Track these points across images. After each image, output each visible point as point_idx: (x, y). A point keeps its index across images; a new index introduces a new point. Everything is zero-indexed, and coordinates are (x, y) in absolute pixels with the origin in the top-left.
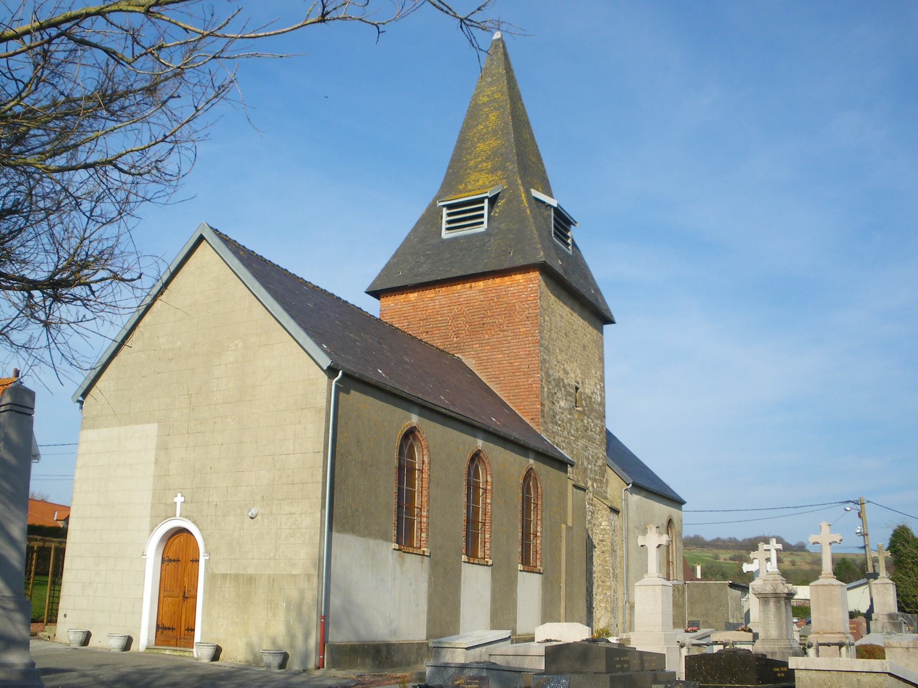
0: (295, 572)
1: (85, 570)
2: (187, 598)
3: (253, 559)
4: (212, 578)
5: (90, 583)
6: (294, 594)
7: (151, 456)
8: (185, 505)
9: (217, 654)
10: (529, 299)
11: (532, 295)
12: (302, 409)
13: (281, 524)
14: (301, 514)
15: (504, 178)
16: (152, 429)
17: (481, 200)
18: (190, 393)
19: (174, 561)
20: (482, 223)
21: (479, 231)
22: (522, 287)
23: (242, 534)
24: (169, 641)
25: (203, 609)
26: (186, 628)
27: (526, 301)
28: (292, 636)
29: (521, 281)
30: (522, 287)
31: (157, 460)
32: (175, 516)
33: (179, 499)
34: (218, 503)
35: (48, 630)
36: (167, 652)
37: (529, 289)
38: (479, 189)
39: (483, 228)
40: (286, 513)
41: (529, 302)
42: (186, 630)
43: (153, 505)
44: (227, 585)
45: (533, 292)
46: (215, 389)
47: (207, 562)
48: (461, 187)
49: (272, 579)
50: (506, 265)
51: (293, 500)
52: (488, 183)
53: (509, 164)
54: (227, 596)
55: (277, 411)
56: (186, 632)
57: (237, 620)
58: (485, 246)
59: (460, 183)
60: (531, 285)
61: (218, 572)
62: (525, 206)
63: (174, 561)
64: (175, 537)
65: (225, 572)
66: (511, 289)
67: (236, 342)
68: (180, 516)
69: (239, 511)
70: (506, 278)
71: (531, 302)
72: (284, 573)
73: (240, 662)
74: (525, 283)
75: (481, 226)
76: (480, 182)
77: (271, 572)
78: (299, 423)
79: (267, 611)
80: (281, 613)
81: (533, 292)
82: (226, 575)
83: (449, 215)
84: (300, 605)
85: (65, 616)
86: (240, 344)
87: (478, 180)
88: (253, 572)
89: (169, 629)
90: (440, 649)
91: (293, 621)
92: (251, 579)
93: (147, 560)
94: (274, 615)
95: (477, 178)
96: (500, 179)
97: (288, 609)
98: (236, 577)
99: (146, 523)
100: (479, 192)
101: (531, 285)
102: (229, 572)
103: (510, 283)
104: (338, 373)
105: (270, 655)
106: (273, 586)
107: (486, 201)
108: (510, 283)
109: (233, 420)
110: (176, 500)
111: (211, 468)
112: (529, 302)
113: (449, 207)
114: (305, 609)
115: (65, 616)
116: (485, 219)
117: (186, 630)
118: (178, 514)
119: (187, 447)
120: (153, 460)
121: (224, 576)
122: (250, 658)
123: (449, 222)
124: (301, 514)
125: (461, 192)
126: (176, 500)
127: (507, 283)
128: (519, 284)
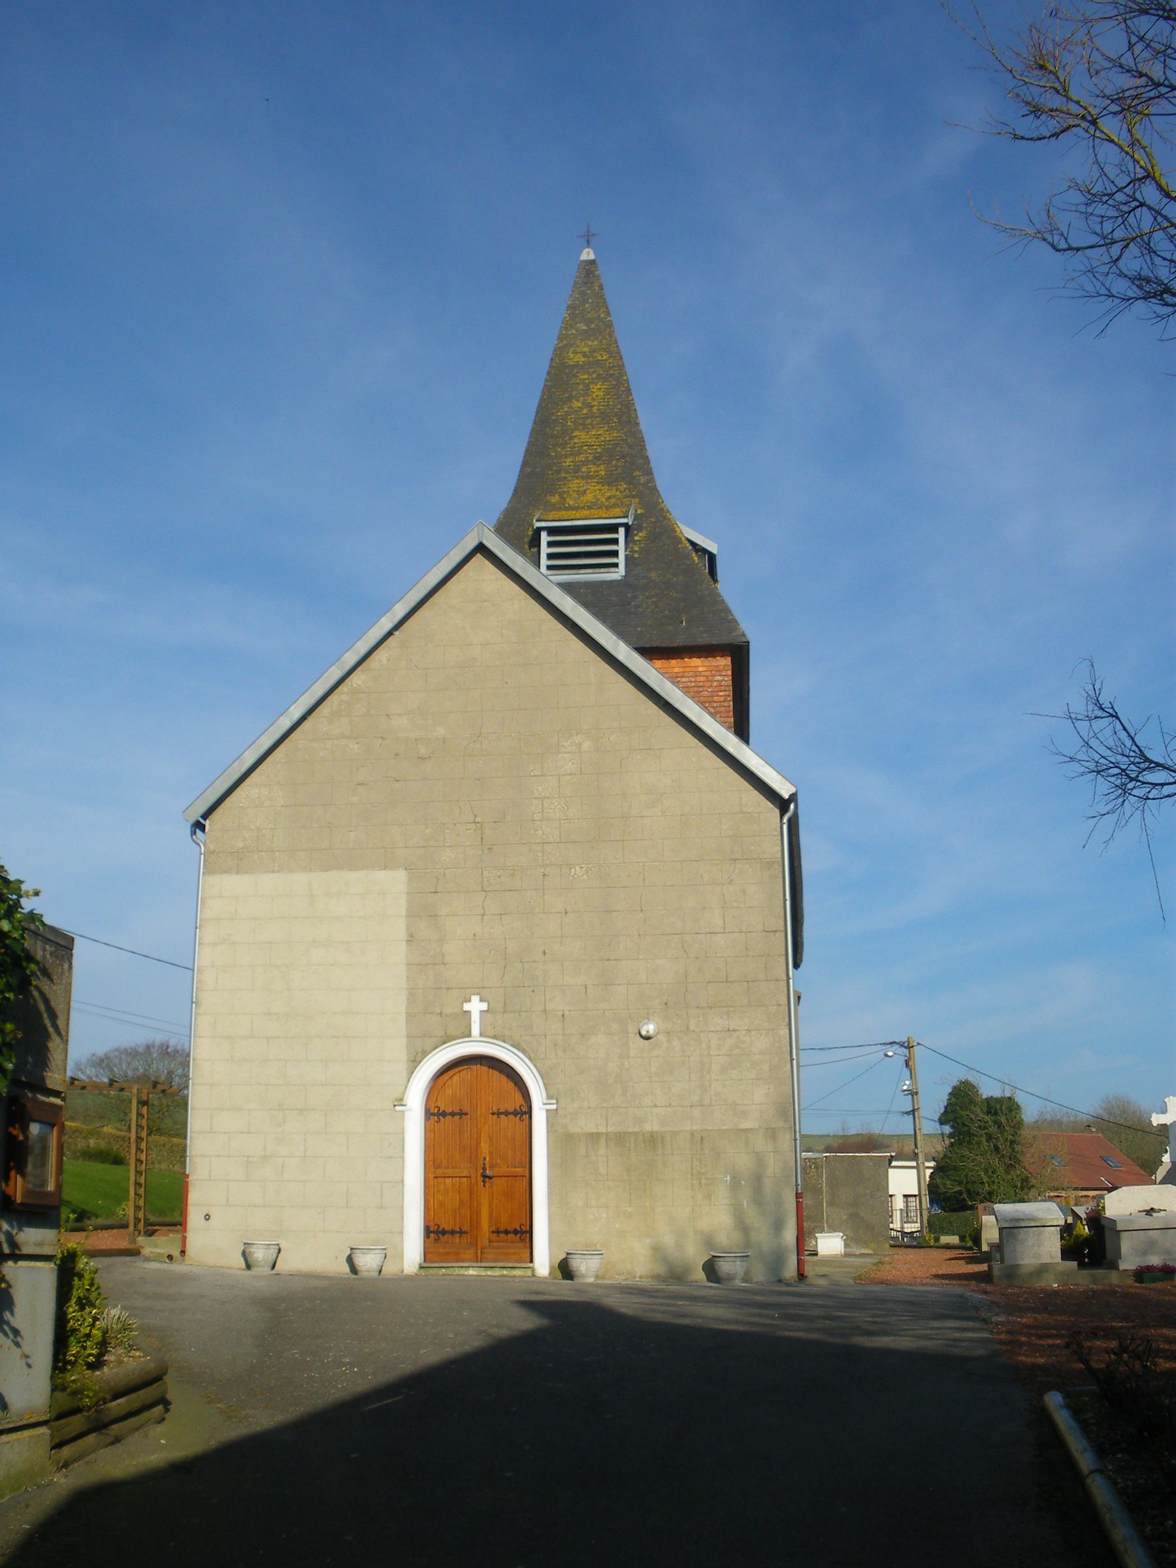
0: (744, 1125)
1: (249, 1132)
2: (490, 1178)
3: (656, 1106)
4: (562, 1142)
5: (264, 1157)
6: (743, 1161)
7: (398, 928)
8: (489, 1016)
9: (565, 1269)
10: (716, 699)
11: (721, 694)
12: (735, 860)
13: (709, 1047)
14: (749, 1031)
15: (634, 497)
16: (395, 881)
17: (614, 528)
18: (478, 819)
19: (453, 1114)
20: (616, 565)
21: (609, 579)
22: (702, 679)
23: (627, 1065)
24: (457, 1254)
25: (550, 1194)
26: (494, 1228)
27: (710, 702)
28: (743, 1227)
29: (701, 669)
30: (702, 679)
31: (411, 935)
32: (469, 1035)
33: (475, 1006)
34: (567, 1012)
35: (159, 1245)
36: (471, 1272)
37: (715, 684)
38: (589, 508)
39: (619, 574)
40: (718, 1029)
41: (715, 705)
42: (493, 1232)
43: (410, 1016)
44: (602, 1151)
45: (722, 688)
46: (537, 817)
47: (551, 1116)
48: (554, 499)
49: (699, 1140)
50: (679, 641)
51: (731, 1009)
52: (604, 500)
53: (638, 473)
54: (603, 1170)
55: (682, 862)
56: (494, 1236)
57: (630, 1209)
58: (629, 604)
59: (552, 494)
60: (719, 678)
61: (578, 1130)
62: (685, 547)
63: (453, 1114)
64: (451, 1073)
65: (594, 1130)
66: (684, 680)
67: (577, 739)
68: (481, 1035)
69: (615, 1026)
70: (674, 662)
71: (718, 704)
72: (724, 1128)
73: (640, 1277)
74: (708, 673)
75: (613, 569)
76: (589, 497)
77: (694, 1128)
78: (731, 882)
79: (693, 1190)
80: (722, 1196)
81: (722, 688)
82: (598, 1135)
83: (551, 544)
84: (757, 1179)
85: (207, 1217)
86: (586, 745)
87: (584, 492)
88: (656, 1128)
89: (453, 1232)
90: (1016, 1231)
91: (747, 1204)
92: (653, 1141)
93: (407, 1114)
94: (708, 1197)
95: (581, 489)
96: (626, 497)
97: (735, 1185)
98: (620, 1139)
99: (398, 1051)
100: (586, 513)
101: (719, 678)
102: (602, 1130)
103: (681, 670)
104: (789, 806)
105: (738, 1259)
106: (702, 1149)
107: (622, 530)
108: (681, 670)
109: (587, 872)
110: (467, 1007)
111: (544, 953)
112: (715, 705)
113: (552, 531)
114: (768, 1185)
115: (207, 1217)
116: (621, 560)
117: (493, 1232)
118: (476, 1030)
119: (484, 915)
120: (402, 934)
121: (594, 1137)
122: (661, 1270)
123: (551, 556)
124: (749, 1031)
125: (554, 507)
126: (467, 1007)
127: (676, 670)
128: (697, 674)
